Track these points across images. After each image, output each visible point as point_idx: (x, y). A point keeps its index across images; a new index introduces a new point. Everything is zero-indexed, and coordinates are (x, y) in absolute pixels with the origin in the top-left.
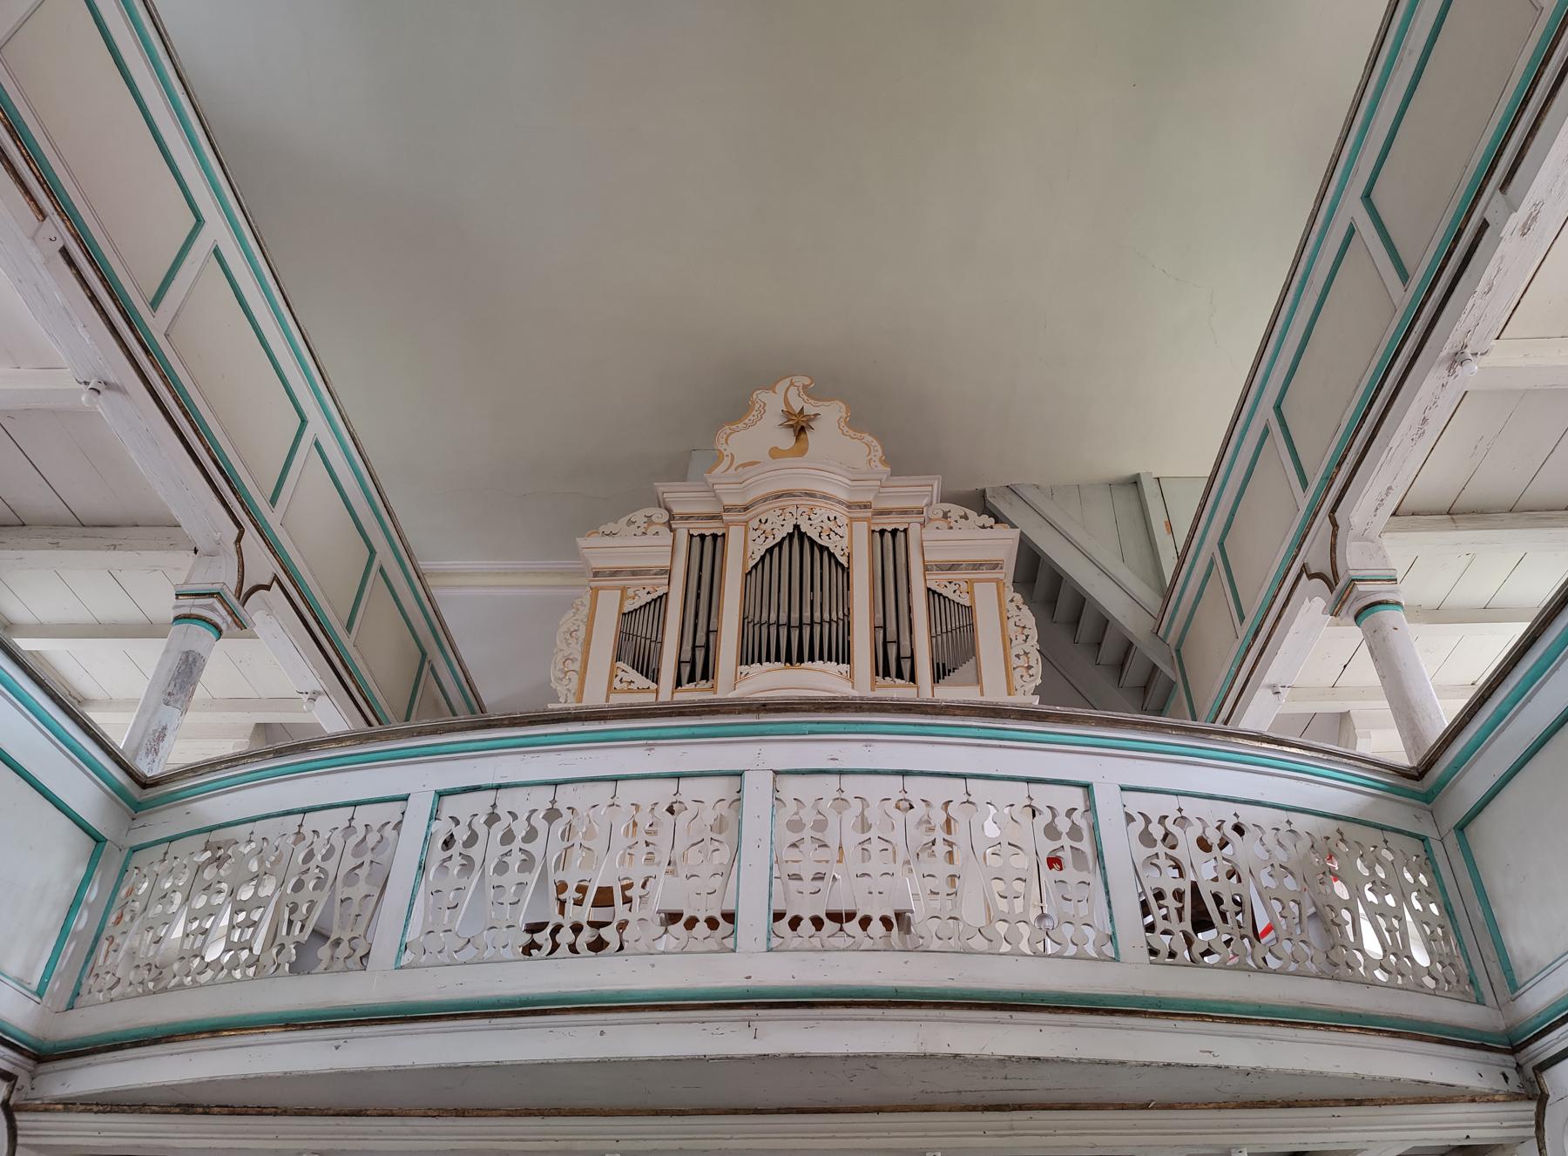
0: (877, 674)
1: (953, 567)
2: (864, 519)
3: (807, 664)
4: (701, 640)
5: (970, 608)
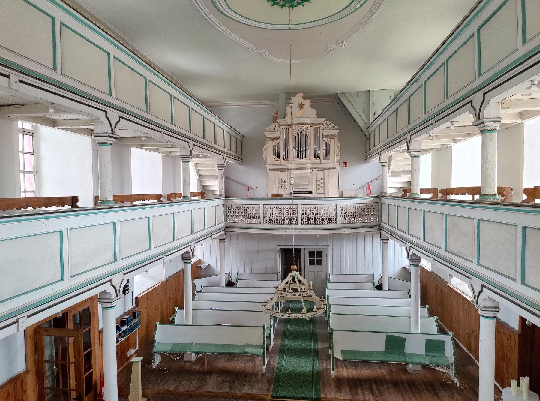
1: (327, 136)
3: (303, 159)
5: (330, 145)
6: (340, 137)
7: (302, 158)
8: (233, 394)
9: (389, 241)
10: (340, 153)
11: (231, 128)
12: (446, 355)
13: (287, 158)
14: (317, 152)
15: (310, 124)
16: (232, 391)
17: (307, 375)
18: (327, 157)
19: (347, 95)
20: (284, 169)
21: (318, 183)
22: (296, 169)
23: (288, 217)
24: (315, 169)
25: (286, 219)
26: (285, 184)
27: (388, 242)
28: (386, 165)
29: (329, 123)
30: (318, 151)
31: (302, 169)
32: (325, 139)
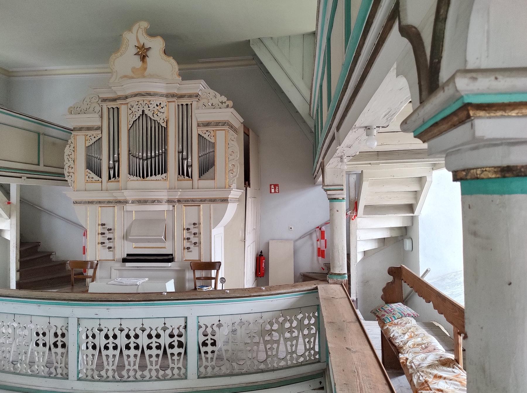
0: (179, 174)
1: (207, 124)
2: (174, 101)
3: (149, 177)
4: (116, 159)
5: (213, 145)
14: (186, 162)
15: (167, 96)
18: (207, 174)
19: (268, 43)
20: (109, 202)
21: (186, 235)
24: (179, 201)
26: (110, 236)
28: (340, 197)
29: (213, 92)
30: (187, 159)
32: (202, 131)
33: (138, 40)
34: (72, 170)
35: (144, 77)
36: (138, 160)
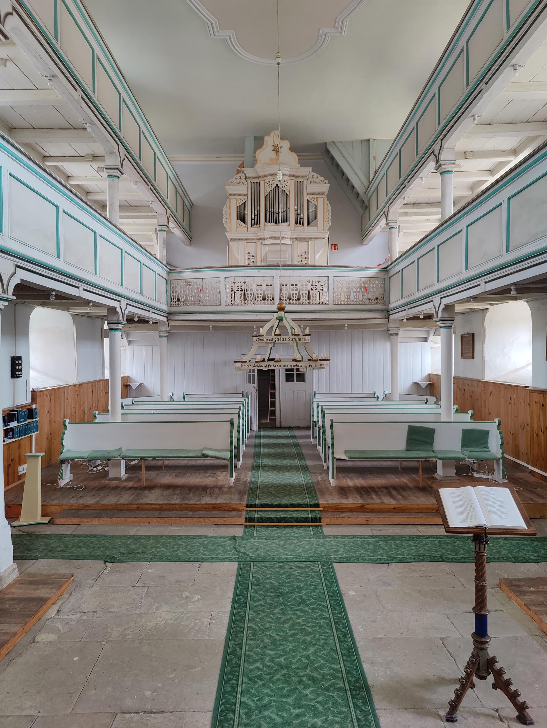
1: (313, 194)
4: (256, 214)
5: (317, 206)
6: (331, 197)
7: (279, 223)
8: (187, 506)
9: (400, 333)
10: (330, 218)
11: (177, 177)
12: (490, 449)
13: (257, 224)
15: (290, 176)
16: (186, 502)
17: (295, 486)
19: (339, 145)
22: (270, 238)
23: (261, 294)
24: (296, 239)
25: (258, 297)
26: (254, 260)
27: (398, 334)
29: (316, 175)
31: (279, 238)
32: (309, 197)
33: (274, 142)
34: (229, 221)
35: (277, 164)
36: (272, 214)
